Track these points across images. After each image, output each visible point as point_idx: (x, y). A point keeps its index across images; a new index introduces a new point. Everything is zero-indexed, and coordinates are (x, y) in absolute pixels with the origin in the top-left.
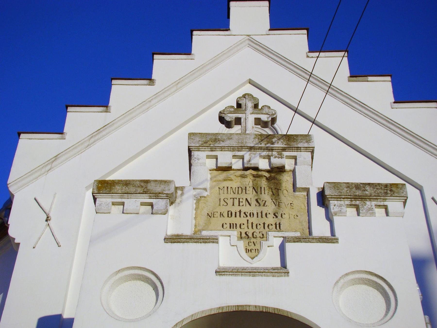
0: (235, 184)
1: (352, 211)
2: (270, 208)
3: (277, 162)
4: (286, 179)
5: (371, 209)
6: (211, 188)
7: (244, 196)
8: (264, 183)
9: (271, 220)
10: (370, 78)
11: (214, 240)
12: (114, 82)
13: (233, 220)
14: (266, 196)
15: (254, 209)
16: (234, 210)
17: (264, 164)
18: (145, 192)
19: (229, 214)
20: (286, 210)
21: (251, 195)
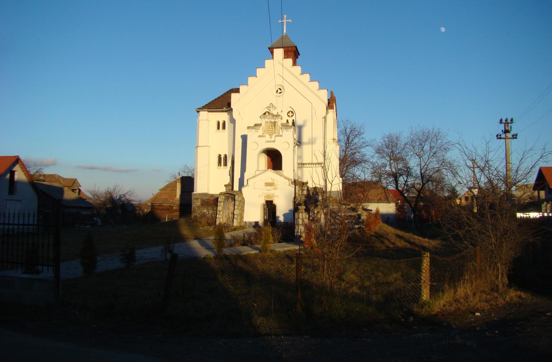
0: (268, 125)
1: (285, 131)
2: (274, 129)
3: (275, 121)
4: (276, 123)
5: (288, 131)
6: (265, 126)
7: (270, 127)
8: (273, 124)
9: (274, 132)
10: (305, 74)
11: (264, 136)
12: (249, 77)
13: (268, 132)
14: (273, 127)
15: (271, 130)
16: (268, 130)
17: (273, 121)
18: (255, 129)
19: (268, 131)
20: (276, 130)
21: (271, 127)
